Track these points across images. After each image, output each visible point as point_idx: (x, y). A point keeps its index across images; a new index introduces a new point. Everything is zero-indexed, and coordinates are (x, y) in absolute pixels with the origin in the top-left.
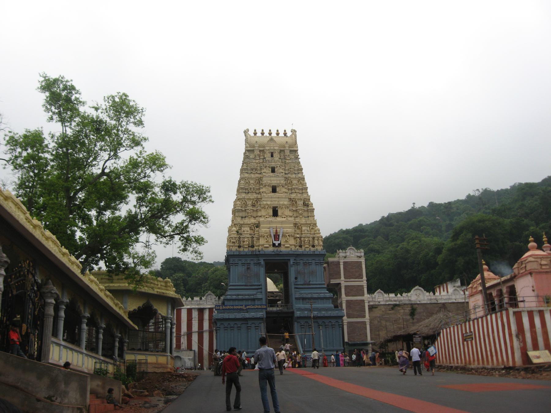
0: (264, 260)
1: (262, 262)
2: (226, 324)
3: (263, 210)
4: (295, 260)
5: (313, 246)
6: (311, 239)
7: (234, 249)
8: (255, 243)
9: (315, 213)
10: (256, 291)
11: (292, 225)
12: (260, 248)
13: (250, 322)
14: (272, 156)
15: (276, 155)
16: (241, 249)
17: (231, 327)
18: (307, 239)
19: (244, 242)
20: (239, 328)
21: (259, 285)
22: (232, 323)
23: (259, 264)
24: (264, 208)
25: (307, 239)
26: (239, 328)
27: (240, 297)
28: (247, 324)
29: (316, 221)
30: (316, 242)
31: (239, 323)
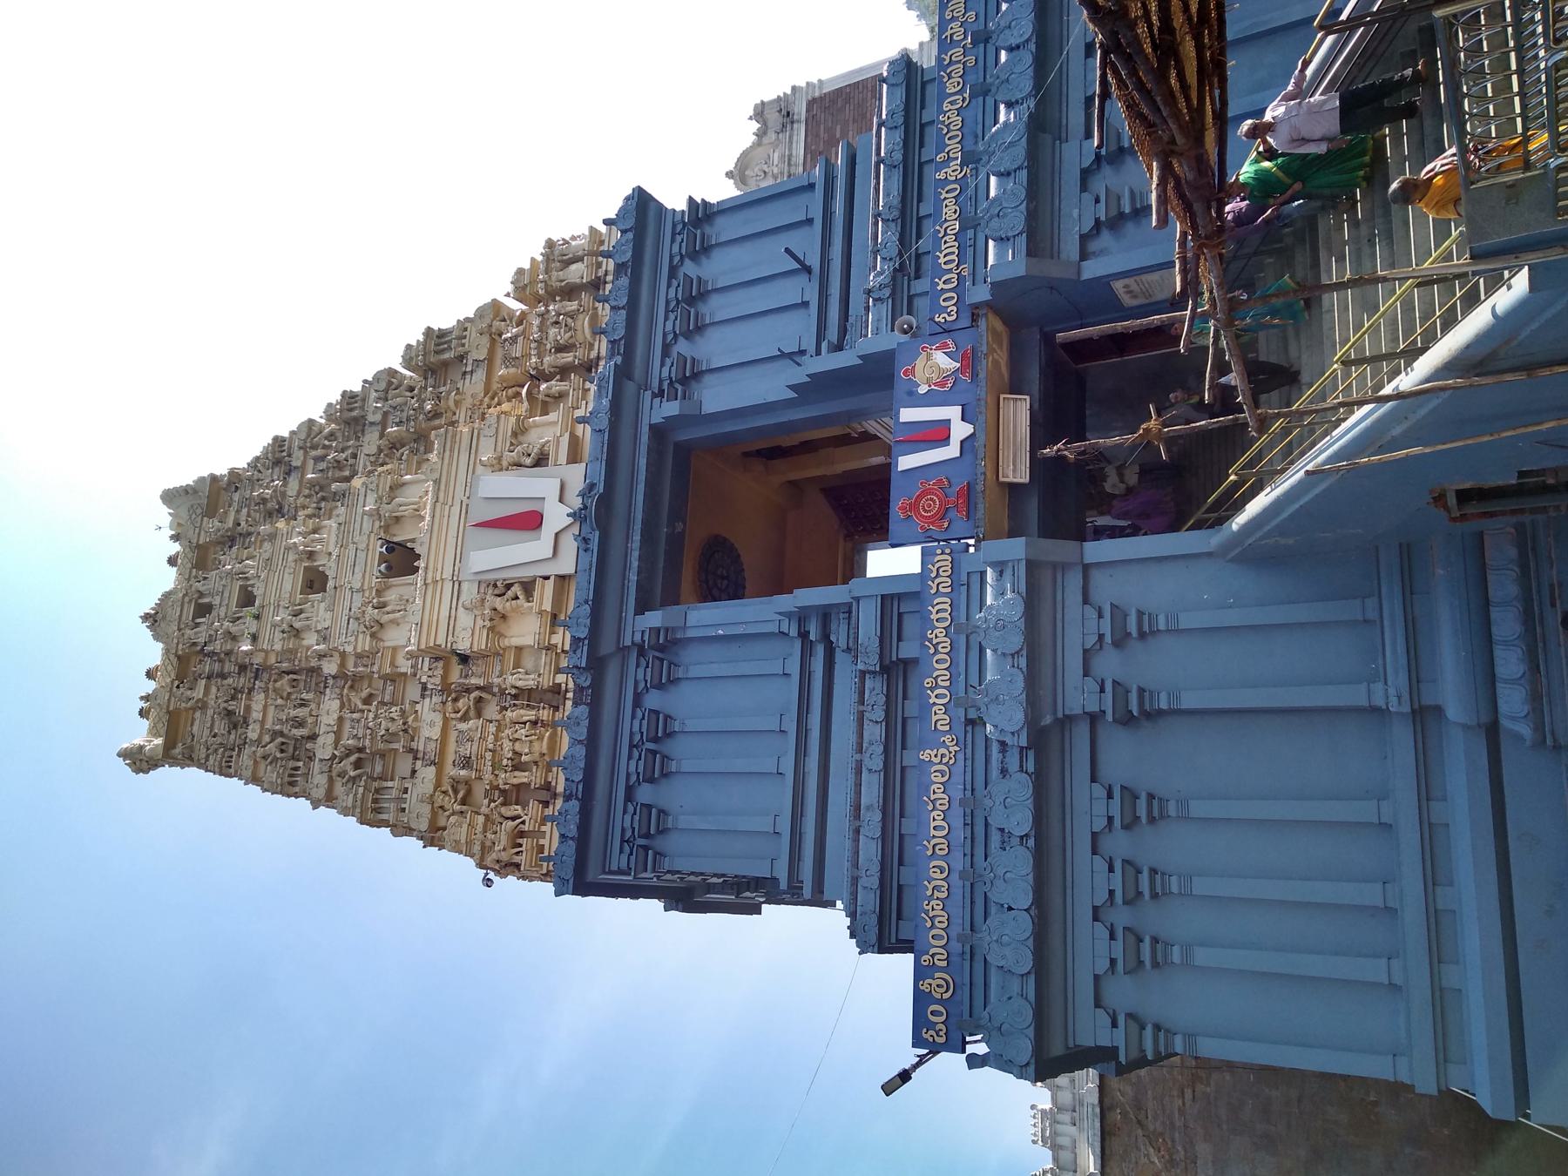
0: (642, 608)
1: (654, 619)
2: (1089, 949)
3: (393, 637)
4: (661, 394)
5: (596, 284)
7: (551, 839)
8: (529, 682)
9: (446, 322)
10: (840, 658)
12: (562, 638)
20: (1140, 809)
21: (804, 635)
22: (1089, 881)
23: (666, 646)
25: (553, 331)
27: (871, 792)
28: (1094, 719)
29: (481, 312)
31: (1087, 807)
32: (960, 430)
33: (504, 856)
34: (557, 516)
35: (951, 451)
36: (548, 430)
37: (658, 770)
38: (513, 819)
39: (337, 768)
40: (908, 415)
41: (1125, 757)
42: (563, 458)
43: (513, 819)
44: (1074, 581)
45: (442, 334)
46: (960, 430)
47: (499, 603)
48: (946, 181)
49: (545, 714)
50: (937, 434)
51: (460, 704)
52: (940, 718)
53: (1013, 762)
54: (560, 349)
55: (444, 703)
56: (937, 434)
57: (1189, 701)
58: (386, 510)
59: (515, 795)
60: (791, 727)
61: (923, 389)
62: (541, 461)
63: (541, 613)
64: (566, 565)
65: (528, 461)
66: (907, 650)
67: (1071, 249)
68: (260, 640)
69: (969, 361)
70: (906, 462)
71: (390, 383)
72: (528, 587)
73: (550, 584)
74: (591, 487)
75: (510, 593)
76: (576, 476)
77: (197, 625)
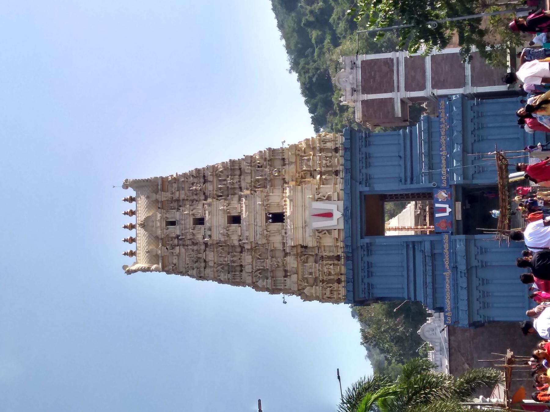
2: (476, 305)
5: (336, 150)
6: (323, 154)
8: (331, 254)
11: (300, 187)
13: (474, 263)
14: (173, 223)
15: (175, 215)
16: (343, 278)
17: (484, 296)
18: (324, 162)
19: (330, 274)
20: (485, 282)
22: (476, 294)
24: (267, 237)
26: (485, 282)
30: (329, 145)
31: (475, 282)
32: (449, 210)
33: (329, 296)
34: (338, 214)
35: (447, 214)
36: (328, 190)
37: (370, 274)
38: (331, 287)
39: (254, 275)
40: (437, 205)
41: (482, 273)
42: (336, 198)
43: (331, 287)
44: (473, 242)
45: (274, 150)
46: (449, 210)
47: (320, 235)
48: (442, 155)
49: (336, 262)
50: (444, 210)
51: (302, 258)
52: (447, 266)
53: (463, 275)
54: (327, 166)
55: (297, 258)
56: (444, 210)
57: (494, 264)
58: (265, 203)
59: (330, 281)
60: (405, 265)
61: (440, 200)
62: (329, 198)
63: (334, 238)
64: (341, 226)
65: (325, 198)
66: (436, 251)
67: (470, 177)
68: (213, 237)
69: (450, 196)
70: (437, 215)
71: (251, 161)
72: (329, 231)
73: (336, 232)
74: (347, 208)
75: (324, 232)
76: (341, 203)
77: (168, 229)
